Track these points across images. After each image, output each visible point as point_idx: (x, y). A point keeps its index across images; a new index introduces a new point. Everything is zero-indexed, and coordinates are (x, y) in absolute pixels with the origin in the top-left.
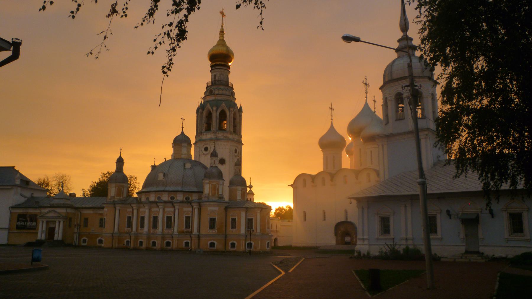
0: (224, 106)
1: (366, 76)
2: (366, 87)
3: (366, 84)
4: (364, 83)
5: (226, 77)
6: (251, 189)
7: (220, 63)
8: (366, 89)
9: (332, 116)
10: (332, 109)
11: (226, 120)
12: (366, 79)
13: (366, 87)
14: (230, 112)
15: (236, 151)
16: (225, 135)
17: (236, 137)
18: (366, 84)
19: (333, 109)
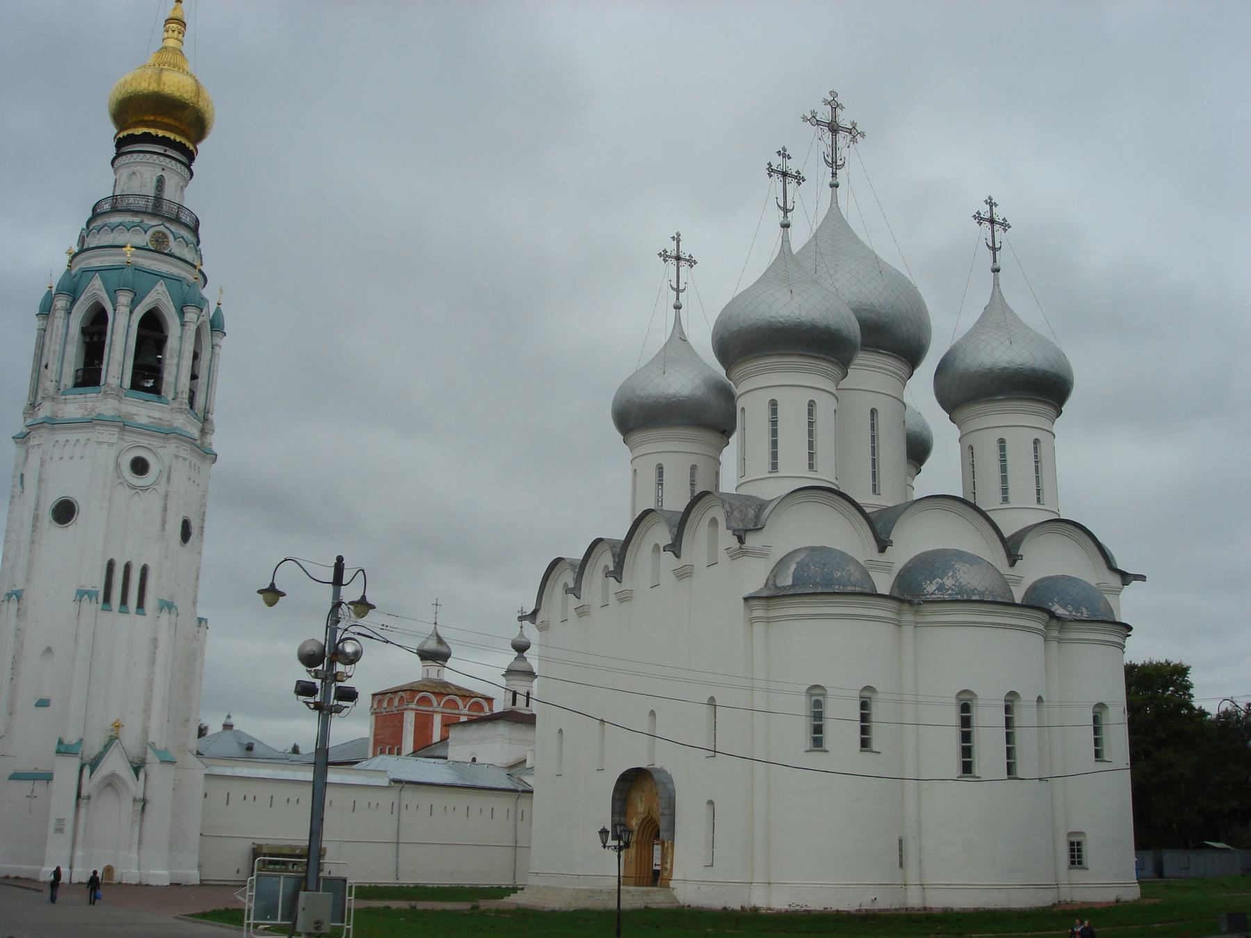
0: (96, 288)
1: (834, 94)
2: (834, 143)
3: (834, 128)
4: (818, 123)
5: (155, 179)
6: (525, 654)
7: (130, 132)
8: (834, 147)
9: (678, 291)
10: (678, 258)
11: (161, 355)
12: (835, 106)
13: (834, 143)
14: (115, 310)
15: (140, 466)
16: (90, 405)
17: (142, 410)
18: (834, 128)
19: (691, 262)
